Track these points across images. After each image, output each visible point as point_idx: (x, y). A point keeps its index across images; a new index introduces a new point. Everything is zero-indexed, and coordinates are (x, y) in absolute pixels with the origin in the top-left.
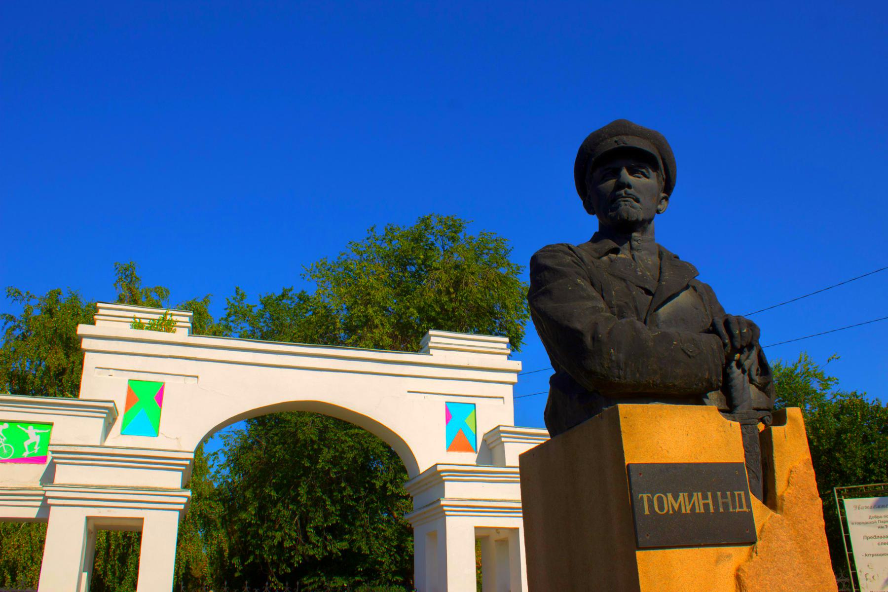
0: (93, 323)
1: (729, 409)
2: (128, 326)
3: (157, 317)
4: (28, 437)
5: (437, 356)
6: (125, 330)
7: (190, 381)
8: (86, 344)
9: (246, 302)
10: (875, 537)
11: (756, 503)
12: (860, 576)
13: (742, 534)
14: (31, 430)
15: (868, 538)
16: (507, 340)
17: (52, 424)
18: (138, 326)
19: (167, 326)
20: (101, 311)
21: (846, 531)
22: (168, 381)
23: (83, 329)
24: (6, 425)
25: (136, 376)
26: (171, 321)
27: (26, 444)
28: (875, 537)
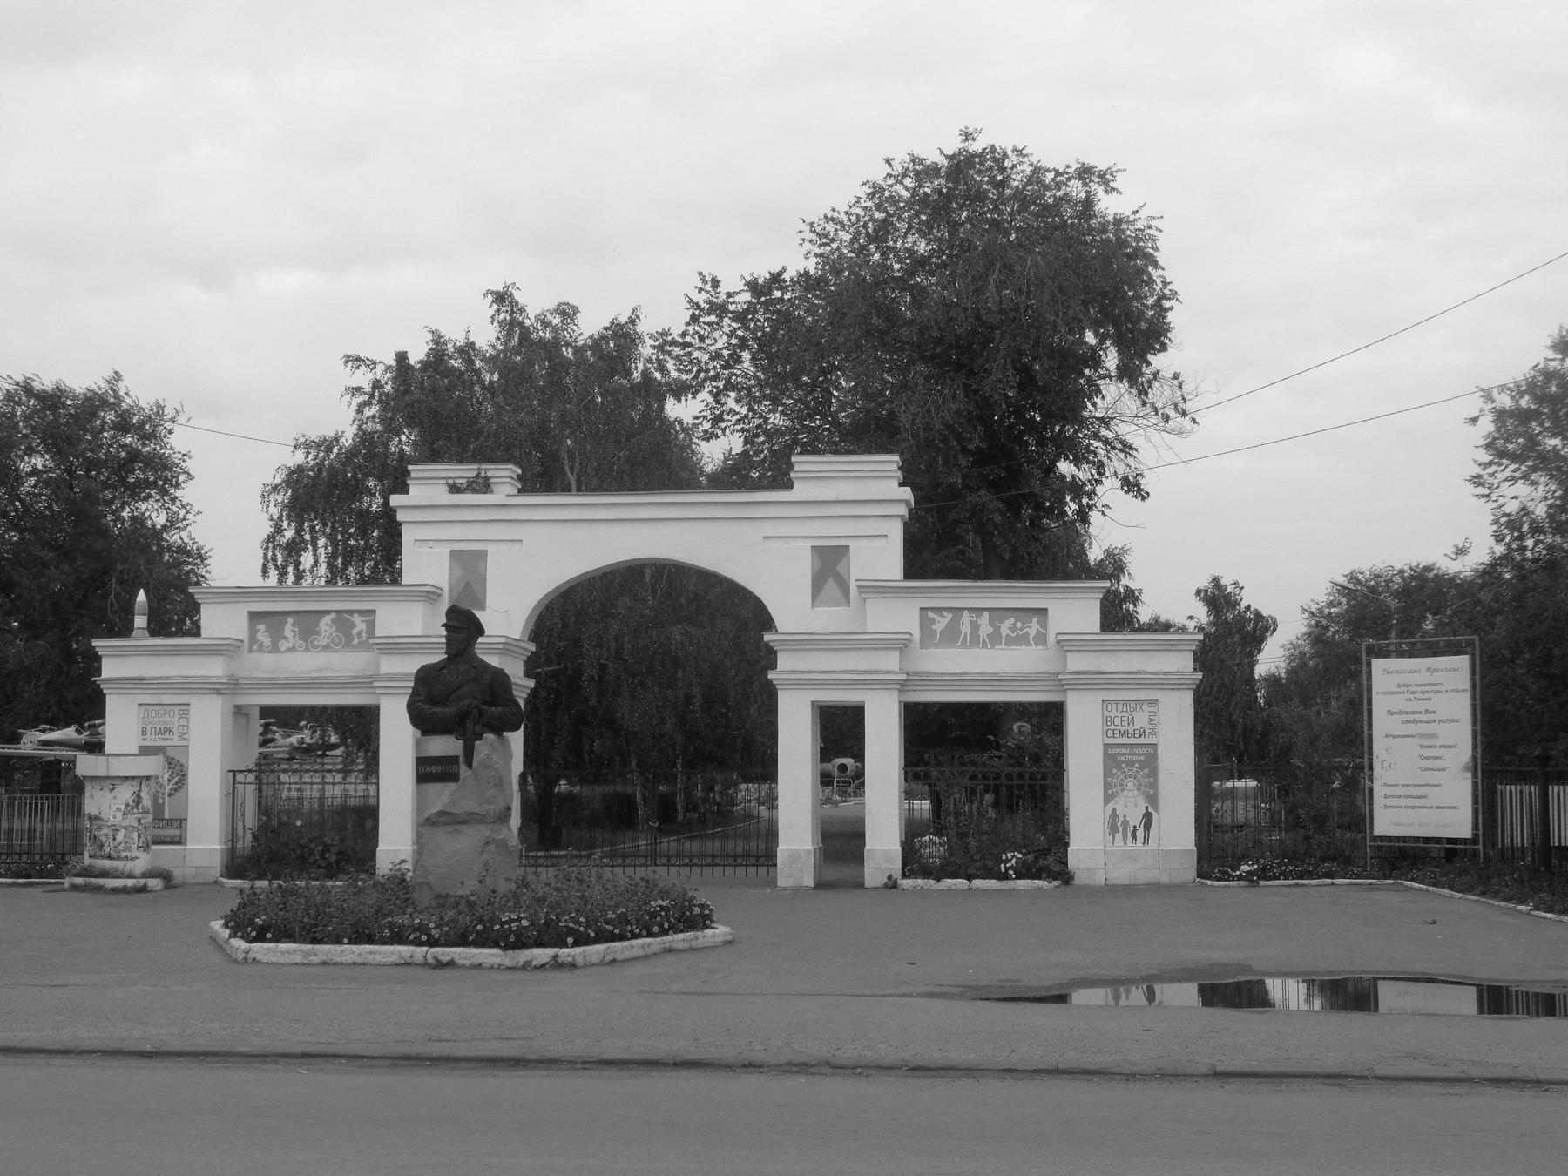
0: (404, 490)
1: (462, 735)
2: (446, 488)
3: (472, 474)
4: (354, 626)
5: (800, 491)
6: (441, 495)
7: (516, 546)
8: (400, 517)
9: (724, 288)
10: (1400, 713)
11: (463, 767)
12: (1376, 764)
13: (454, 777)
14: (357, 619)
15: (1391, 713)
16: (896, 458)
17: (373, 612)
18: (454, 489)
19: (483, 485)
20: (413, 475)
21: (1370, 703)
22: (490, 548)
23: (396, 500)
24: (333, 615)
25: (457, 546)
26: (487, 479)
27: (354, 632)
28: (1400, 713)
